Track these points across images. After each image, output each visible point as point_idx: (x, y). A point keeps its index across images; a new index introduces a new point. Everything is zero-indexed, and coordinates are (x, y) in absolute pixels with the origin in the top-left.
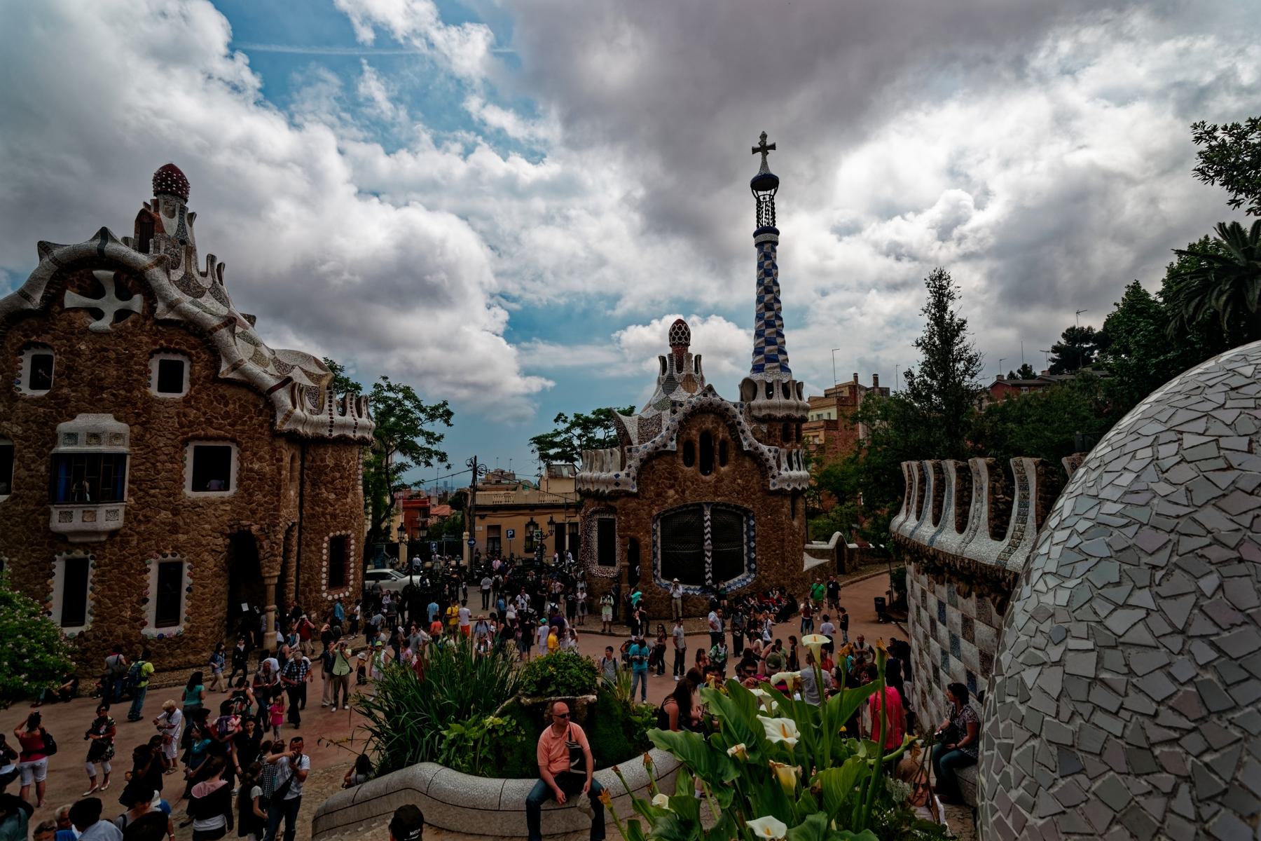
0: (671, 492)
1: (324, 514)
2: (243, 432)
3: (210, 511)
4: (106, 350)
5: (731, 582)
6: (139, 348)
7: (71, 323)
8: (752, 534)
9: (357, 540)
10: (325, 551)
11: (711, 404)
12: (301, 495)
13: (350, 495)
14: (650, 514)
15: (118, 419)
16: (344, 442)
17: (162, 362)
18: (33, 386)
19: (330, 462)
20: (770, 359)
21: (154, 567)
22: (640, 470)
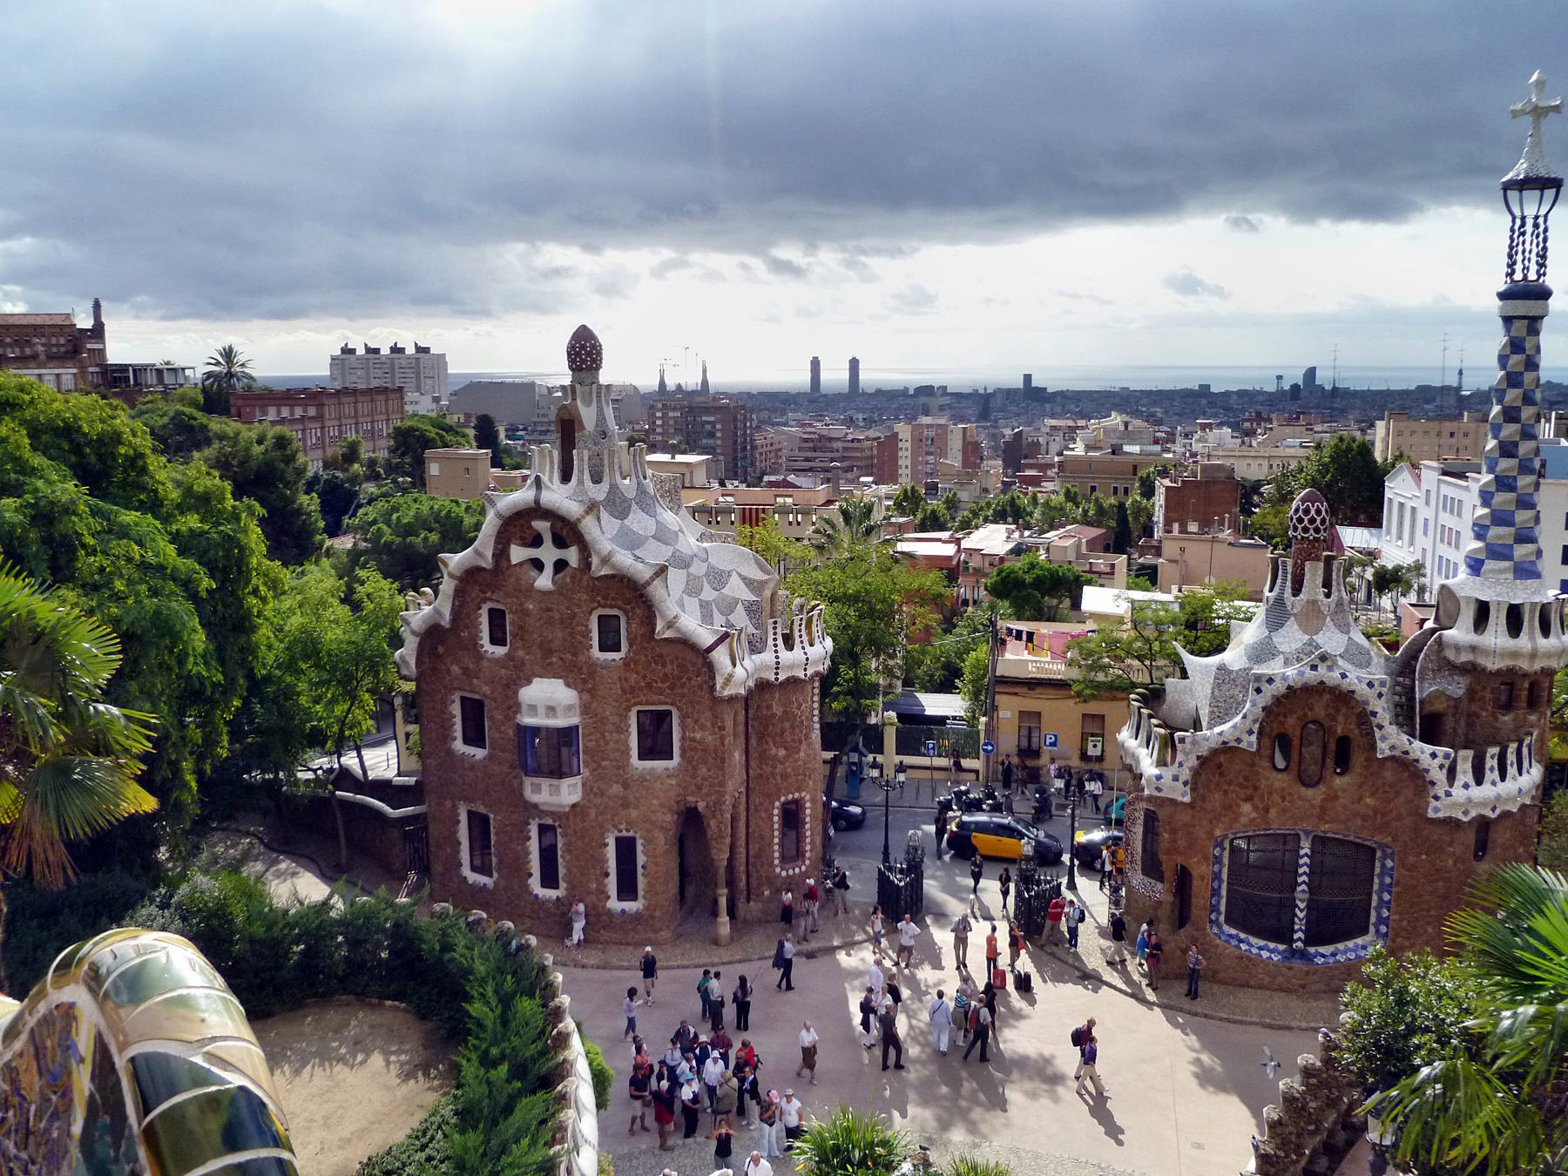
0: (1246, 808)
1: (773, 774)
2: (683, 696)
3: (658, 785)
4: (549, 610)
5: (1341, 946)
6: (579, 606)
7: (518, 579)
8: (1388, 880)
9: (813, 801)
10: (776, 819)
11: (1322, 683)
12: (747, 752)
13: (803, 747)
14: (1210, 834)
15: (568, 685)
16: (793, 682)
17: (600, 617)
18: (494, 641)
19: (777, 710)
20: (1497, 552)
21: (611, 841)
22: (1196, 773)
